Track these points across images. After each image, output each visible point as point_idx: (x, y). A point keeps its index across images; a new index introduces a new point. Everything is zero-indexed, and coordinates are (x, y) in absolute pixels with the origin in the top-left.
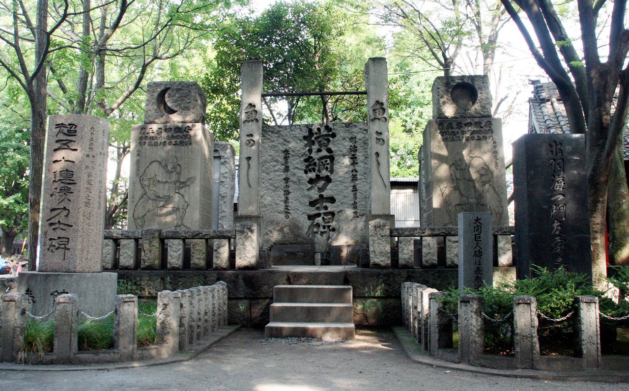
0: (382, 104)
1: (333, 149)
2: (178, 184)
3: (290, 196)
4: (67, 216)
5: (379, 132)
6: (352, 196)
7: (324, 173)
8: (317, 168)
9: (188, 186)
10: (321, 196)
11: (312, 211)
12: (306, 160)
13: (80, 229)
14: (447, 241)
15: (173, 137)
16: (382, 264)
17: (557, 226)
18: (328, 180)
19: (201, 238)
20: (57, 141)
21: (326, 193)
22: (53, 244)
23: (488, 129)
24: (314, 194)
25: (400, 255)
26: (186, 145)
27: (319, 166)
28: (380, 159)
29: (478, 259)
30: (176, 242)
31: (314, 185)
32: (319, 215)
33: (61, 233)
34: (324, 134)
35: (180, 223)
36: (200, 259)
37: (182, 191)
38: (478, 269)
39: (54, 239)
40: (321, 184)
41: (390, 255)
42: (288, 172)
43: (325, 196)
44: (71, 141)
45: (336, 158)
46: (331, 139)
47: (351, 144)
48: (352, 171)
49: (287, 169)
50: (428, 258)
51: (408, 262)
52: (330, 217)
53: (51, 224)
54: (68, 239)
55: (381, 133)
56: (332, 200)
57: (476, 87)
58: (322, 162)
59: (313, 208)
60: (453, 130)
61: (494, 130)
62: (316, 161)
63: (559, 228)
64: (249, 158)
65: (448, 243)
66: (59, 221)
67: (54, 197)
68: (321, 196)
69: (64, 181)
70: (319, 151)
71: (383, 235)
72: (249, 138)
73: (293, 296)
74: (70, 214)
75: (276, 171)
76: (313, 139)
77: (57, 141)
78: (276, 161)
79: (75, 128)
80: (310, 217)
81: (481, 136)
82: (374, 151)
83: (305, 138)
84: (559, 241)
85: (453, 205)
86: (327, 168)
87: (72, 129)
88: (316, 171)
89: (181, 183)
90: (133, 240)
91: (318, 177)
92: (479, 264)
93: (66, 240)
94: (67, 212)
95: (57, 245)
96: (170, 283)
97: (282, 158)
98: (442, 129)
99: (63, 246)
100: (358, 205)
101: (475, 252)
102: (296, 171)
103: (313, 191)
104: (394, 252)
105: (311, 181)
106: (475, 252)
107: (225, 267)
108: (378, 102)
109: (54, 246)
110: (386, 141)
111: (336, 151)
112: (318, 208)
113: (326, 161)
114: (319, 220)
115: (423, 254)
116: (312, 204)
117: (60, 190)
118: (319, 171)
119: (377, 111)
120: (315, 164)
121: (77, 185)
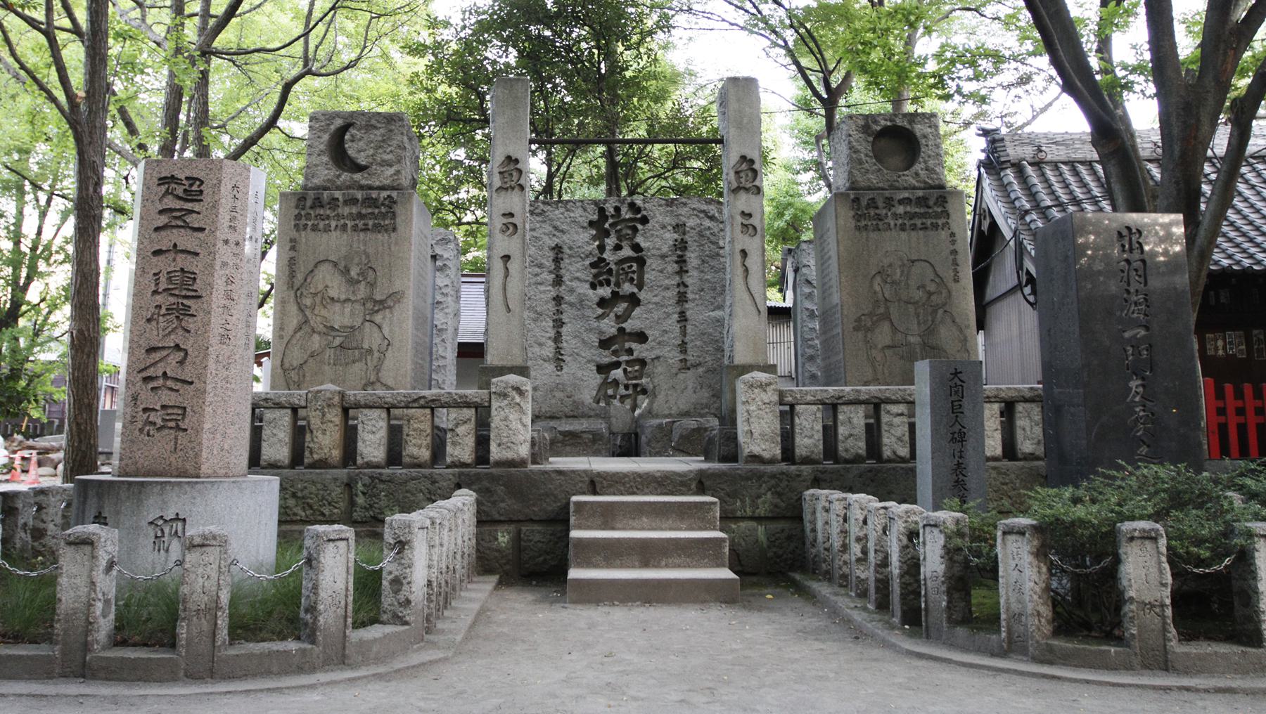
0: (752, 162)
1: (643, 245)
2: (369, 305)
3: (564, 330)
4: (181, 363)
5: (747, 212)
6: (678, 330)
7: (627, 288)
8: (613, 280)
9: (390, 307)
10: (621, 330)
11: (606, 357)
12: (593, 265)
13: (209, 388)
14: (883, 413)
15: (360, 216)
16: (766, 455)
17: (1137, 387)
18: (634, 301)
20: (161, 212)
21: (629, 326)
22: (151, 419)
23: (939, 210)
24: (609, 326)
25: (798, 440)
27: (618, 274)
28: (748, 262)
29: (957, 446)
30: (375, 413)
31: (608, 311)
32: (617, 365)
33: (167, 398)
34: (627, 217)
35: (373, 378)
37: (378, 318)
38: (959, 464)
39: (154, 410)
40: (621, 307)
41: (779, 439)
42: (560, 285)
43: (628, 331)
44: (191, 212)
45: (649, 262)
46: (640, 227)
47: (676, 236)
48: (678, 285)
49: (558, 281)
50: (850, 442)
51: (813, 452)
52: (637, 368)
53: (147, 379)
54: (185, 408)
55: (750, 215)
56: (641, 337)
57: (918, 134)
58: (623, 269)
59: (607, 352)
60: (877, 211)
61: (951, 211)
62: (613, 267)
64: (506, 258)
65: (885, 418)
66: (165, 373)
67: (154, 323)
68: (621, 330)
69: (177, 292)
70: (618, 248)
71: (767, 401)
72: (505, 221)
73: (608, 516)
74: (189, 359)
75: (541, 284)
76: (607, 226)
77: (161, 212)
78: (540, 266)
79: (199, 186)
81: (929, 222)
82: (738, 247)
83: (591, 224)
85: (880, 346)
86: (632, 280)
87: (195, 188)
88: (612, 285)
89: (376, 302)
90: (289, 411)
91: (615, 294)
92: (961, 457)
93: (180, 412)
94: (182, 354)
95: (159, 422)
96: (364, 494)
97: (550, 259)
98: (858, 209)
99: (172, 424)
100: (689, 346)
101: (953, 434)
102: (574, 284)
103: (606, 321)
104: (787, 438)
105: (602, 303)
106: (953, 434)
107: (469, 461)
108: (743, 158)
109: (155, 424)
110: (759, 229)
111: (649, 250)
112: (615, 353)
113: (631, 266)
114: (618, 373)
115: (840, 437)
116: (605, 344)
117: (167, 309)
118: (618, 284)
119: (742, 175)
120: (610, 271)
121: (204, 299)
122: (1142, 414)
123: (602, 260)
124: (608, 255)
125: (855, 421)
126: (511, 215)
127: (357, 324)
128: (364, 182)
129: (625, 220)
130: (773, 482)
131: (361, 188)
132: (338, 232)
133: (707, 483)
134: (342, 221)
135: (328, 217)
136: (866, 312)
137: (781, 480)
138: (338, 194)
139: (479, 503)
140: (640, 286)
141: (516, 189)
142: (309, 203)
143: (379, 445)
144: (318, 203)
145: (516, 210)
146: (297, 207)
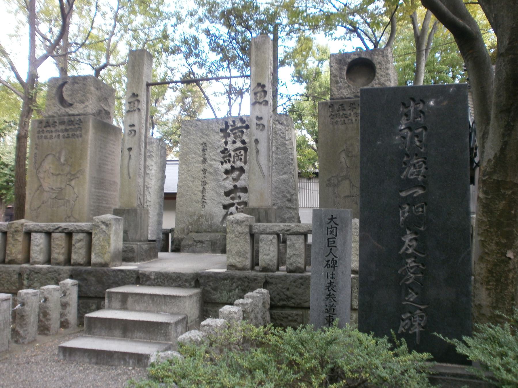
1: (246, 140)
2: (69, 176)
5: (259, 116)
7: (239, 164)
8: (232, 160)
9: (78, 178)
10: (235, 186)
11: (227, 200)
12: (223, 152)
15: (66, 130)
16: (240, 265)
17: (411, 240)
18: (242, 170)
19: (60, 232)
21: (239, 184)
24: (229, 184)
25: (261, 256)
26: (77, 137)
27: (234, 157)
31: (229, 176)
32: (232, 205)
34: (239, 126)
35: (70, 215)
36: (59, 254)
37: (73, 183)
38: (331, 283)
40: (236, 174)
42: (205, 163)
43: (238, 186)
46: (245, 130)
49: (205, 161)
50: (292, 260)
51: (269, 265)
52: (242, 206)
55: (261, 118)
56: (245, 190)
58: (237, 154)
59: (228, 198)
60: (345, 112)
62: (233, 153)
63: (414, 243)
64: (130, 149)
68: (235, 186)
70: (234, 142)
71: (241, 232)
72: (130, 129)
75: (195, 163)
76: (229, 131)
78: (195, 153)
80: (226, 207)
82: (254, 138)
83: (222, 130)
85: (342, 196)
88: (231, 162)
89: (72, 175)
92: (333, 278)
96: (28, 279)
97: (201, 150)
98: (332, 112)
101: (328, 261)
102: (213, 163)
103: (228, 181)
105: (227, 172)
106: (328, 261)
107: (82, 263)
110: (266, 126)
112: (233, 199)
115: (287, 256)
116: (227, 194)
119: (259, 95)
120: (230, 155)
122: (414, 264)
123: (226, 149)
124: (230, 147)
125: (297, 246)
126: (133, 125)
127: (63, 186)
128: (70, 112)
129: (237, 128)
130: (239, 283)
131: (69, 115)
132: (56, 139)
133: (201, 281)
134: (58, 133)
135: (52, 132)
136: (334, 175)
137: (244, 282)
138: (56, 119)
139: (79, 286)
140: (245, 163)
141: (137, 111)
142: (44, 124)
143: (40, 252)
144: (48, 125)
145: (136, 123)
146: (38, 127)
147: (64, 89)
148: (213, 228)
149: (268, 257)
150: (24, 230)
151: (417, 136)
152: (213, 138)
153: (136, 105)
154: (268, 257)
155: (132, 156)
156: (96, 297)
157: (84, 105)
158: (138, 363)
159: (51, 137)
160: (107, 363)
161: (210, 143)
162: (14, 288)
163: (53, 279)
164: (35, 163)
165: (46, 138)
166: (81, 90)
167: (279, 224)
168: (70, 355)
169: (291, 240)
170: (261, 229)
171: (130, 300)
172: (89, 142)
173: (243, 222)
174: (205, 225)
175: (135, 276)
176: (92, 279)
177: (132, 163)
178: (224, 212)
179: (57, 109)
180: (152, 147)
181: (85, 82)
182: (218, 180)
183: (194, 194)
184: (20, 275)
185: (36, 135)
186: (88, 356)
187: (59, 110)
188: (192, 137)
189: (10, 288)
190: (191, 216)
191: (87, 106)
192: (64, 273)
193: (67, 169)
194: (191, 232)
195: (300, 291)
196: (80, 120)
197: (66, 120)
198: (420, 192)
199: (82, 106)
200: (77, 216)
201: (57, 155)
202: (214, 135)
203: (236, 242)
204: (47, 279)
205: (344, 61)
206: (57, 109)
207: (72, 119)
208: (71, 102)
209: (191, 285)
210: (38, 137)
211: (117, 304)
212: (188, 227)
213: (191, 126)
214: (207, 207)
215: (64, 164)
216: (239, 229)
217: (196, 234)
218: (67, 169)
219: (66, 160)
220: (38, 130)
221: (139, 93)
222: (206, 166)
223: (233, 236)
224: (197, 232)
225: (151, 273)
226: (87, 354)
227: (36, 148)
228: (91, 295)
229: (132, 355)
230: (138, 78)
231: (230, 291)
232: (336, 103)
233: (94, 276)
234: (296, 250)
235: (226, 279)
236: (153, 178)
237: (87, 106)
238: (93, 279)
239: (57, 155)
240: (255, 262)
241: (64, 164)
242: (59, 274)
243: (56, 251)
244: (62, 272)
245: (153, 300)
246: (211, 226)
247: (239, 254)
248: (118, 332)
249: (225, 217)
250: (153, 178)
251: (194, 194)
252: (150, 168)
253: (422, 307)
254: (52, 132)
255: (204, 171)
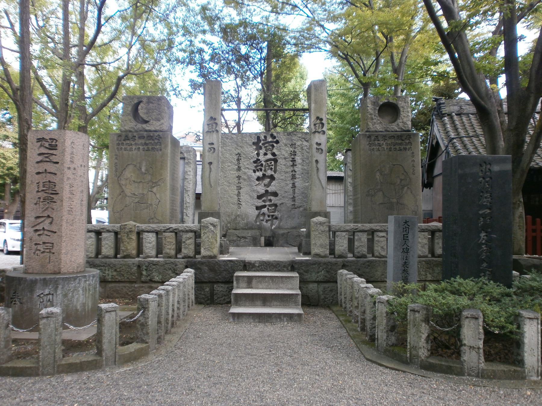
0: (321, 120)
1: (276, 153)
2: (150, 184)
3: (241, 191)
4: (51, 223)
6: (291, 191)
7: (269, 172)
8: (263, 169)
9: (159, 185)
12: (255, 162)
13: (63, 235)
14: (375, 236)
15: (146, 144)
16: (322, 254)
18: (272, 178)
19: (171, 232)
20: (40, 154)
21: (270, 189)
22: (38, 248)
23: (407, 141)
24: (261, 189)
26: (157, 150)
28: (319, 165)
29: (405, 254)
30: (150, 235)
32: (264, 206)
33: (44, 238)
35: (153, 217)
36: (170, 249)
37: (155, 190)
38: (405, 262)
39: (39, 244)
40: (267, 181)
41: (328, 247)
43: (270, 191)
44: (53, 154)
45: (279, 161)
46: (275, 145)
47: (291, 149)
48: (292, 171)
49: (239, 169)
50: (359, 250)
51: (343, 253)
52: (273, 208)
53: (36, 231)
54: (53, 243)
55: (320, 144)
56: (275, 194)
57: (399, 106)
59: (260, 201)
60: (379, 142)
61: (413, 143)
62: (264, 163)
63: (485, 237)
64: (210, 163)
65: (376, 239)
66: (43, 229)
67: (38, 205)
69: (47, 191)
70: (265, 154)
72: (210, 146)
73: (249, 281)
74: (54, 222)
76: (261, 144)
77: (40, 154)
78: (231, 162)
79: (56, 142)
80: (258, 208)
81: (402, 147)
82: (315, 159)
83: (254, 143)
84: (485, 248)
85: (378, 203)
86: (271, 169)
87: (53, 143)
89: (153, 183)
90: (113, 234)
91: (264, 175)
93: (51, 245)
94: (51, 219)
95: (42, 250)
96: (146, 270)
97: (236, 159)
99: (48, 251)
100: (297, 198)
101: (403, 249)
102: (246, 171)
104: (332, 245)
105: (258, 179)
106: (403, 249)
108: (318, 118)
109: (40, 250)
111: (279, 155)
112: (264, 201)
113: (271, 163)
114: (265, 210)
115: (355, 247)
117: (44, 199)
118: (265, 171)
119: (317, 125)
120: (262, 165)
121: (59, 195)
123: (258, 160)
124: (262, 158)
125: (362, 240)
126: (213, 144)
127: (145, 192)
128: (147, 128)
129: (269, 142)
130: (324, 266)
131: (146, 131)
132: (136, 151)
133: (296, 266)
134: (138, 146)
135: (131, 145)
136: (372, 188)
137: (328, 265)
138: (135, 134)
139: (195, 274)
140: (275, 172)
141: (215, 132)
142: (123, 138)
143: (153, 248)
144: (127, 138)
145: (215, 142)
146: (117, 140)
147: (140, 107)
148: (249, 226)
149: (343, 248)
150: (136, 230)
151: (487, 182)
152: (247, 150)
153: (214, 127)
154: (343, 248)
155: (212, 169)
156: (210, 282)
157: (159, 123)
158: (290, 319)
159: (131, 150)
160: (267, 321)
161: (244, 154)
162: (134, 277)
163: (170, 269)
164: (116, 171)
165: (126, 149)
166: (156, 109)
167: (349, 224)
168: (238, 318)
169: (358, 236)
170: (337, 228)
171: (254, 281)
172: (169, 155)
173: (325, 223)
174: (242, 223)
175: (242, 264)
176: (205, 268)
177: (213, 175)
178: (257, 212)
179: (132, 125)
180: (190, 155)
181: (160, 103)
182: (251, 186)
183: (231, 197)
184: (139, 267)
185: (116, 147)
186: (252, 318)
187: (136, 126)
188: (228, 148)
189: (130, 278)
190: (229, 216)
191: (163, 124)
192: (181, 264)
193: (149, 177)
194: (230, 229)
195: (367, 270)
196: (159, 135)
197: (145, 136)
198: (489, 211)
199: (158, 123)
200: (160, 218)
201: (138, 165)
202: (247, 148)
203: (319, 237)
204: (165, 269)
205: (377, 103)
206: (132, 125)
207: (152, 135)
208: (147, 120)
209: (288, 269)
210: (118, 148)
211: (245, 285)
212: (227, 225)
213: (227, 138)
214: (242, 208)
215: (145, 174)
216: (322, 228)
217: (234, 231)
218: (149, 177)
219: (146, 170)
220: (117, 142)
221: (216, 117)
222: (240, 173)
223: (317, 233)
224: (235, 229)
225: (256, 262)
226: (251, 317)
227: (116, 158)
228: (205, 281)
229: (285, 315)
230: (215, 105)
231: (318, 272)
232: (373, 135)
233: (207, 266)
234: (362, 242)
235: (315, 264)
236: (191, 182)
237: (163, 124)
238: (207, 268)
239: (138, 165)
240: (332, 252)
241: (145, 174)
242: (176, 265)
243: (168, 247)
244: (178, 264)
245: (273, 281)
246: (247, 224)
247: (321, 246)
248: (259, 303)
249: (258, 216)
250: (191, 182)
251: (231, 197)
252: (189, 173)
253: (490, 270)
254: (131, 145)
255: (239, 177)
